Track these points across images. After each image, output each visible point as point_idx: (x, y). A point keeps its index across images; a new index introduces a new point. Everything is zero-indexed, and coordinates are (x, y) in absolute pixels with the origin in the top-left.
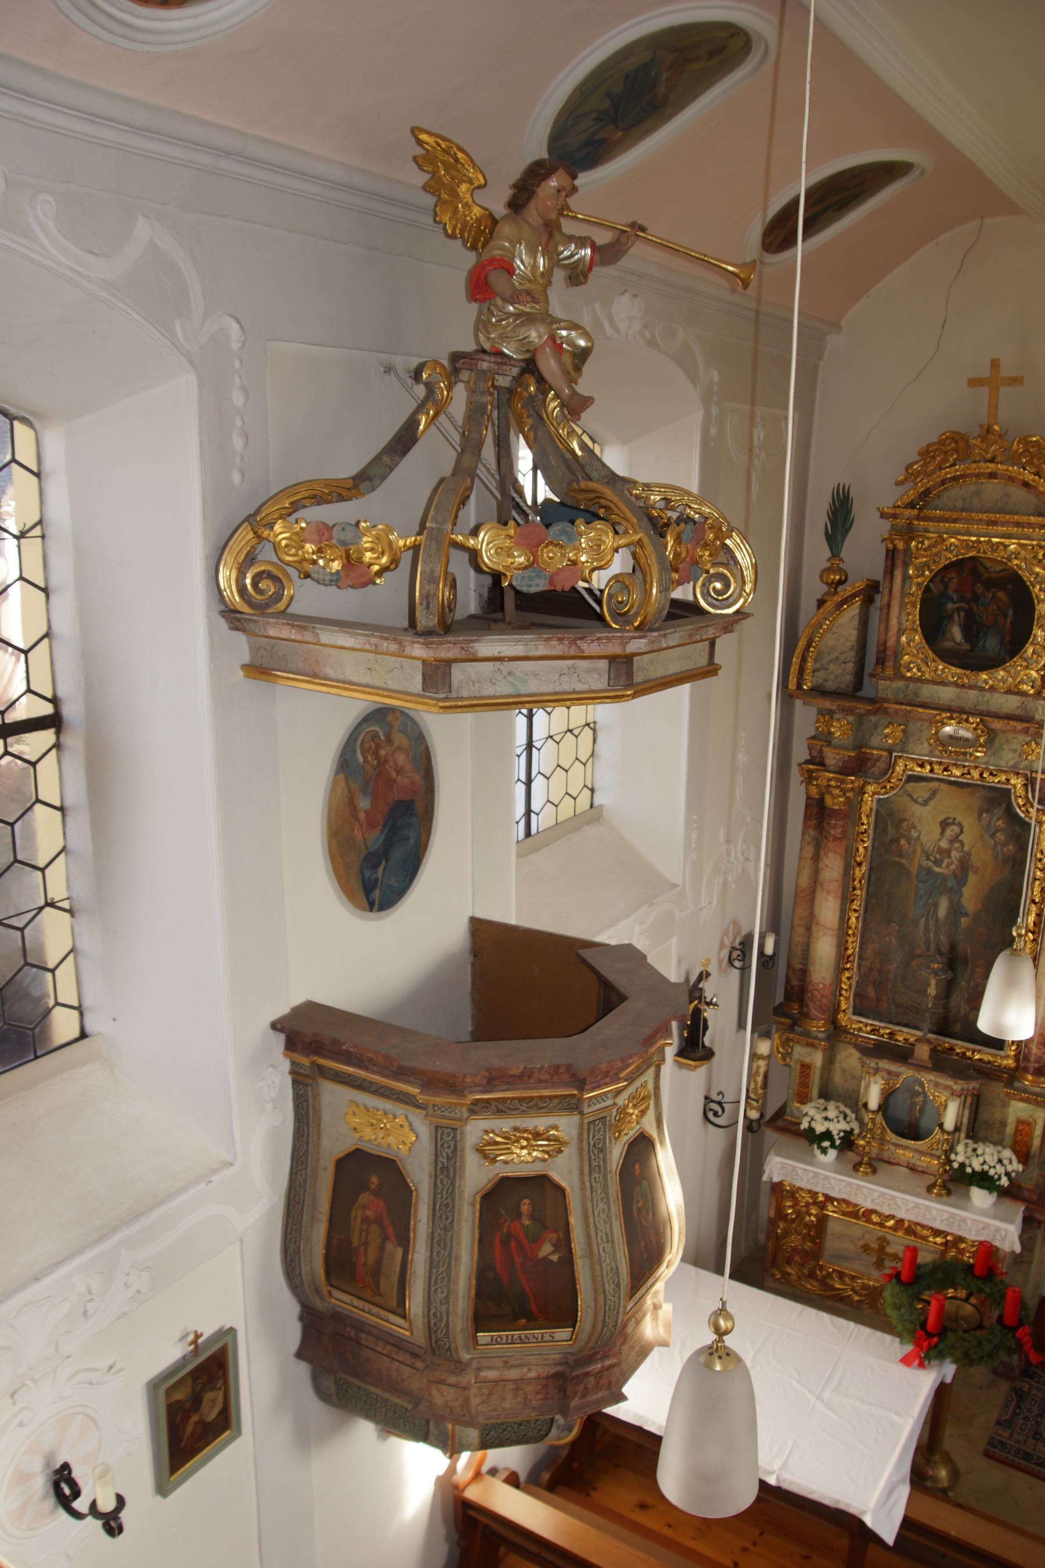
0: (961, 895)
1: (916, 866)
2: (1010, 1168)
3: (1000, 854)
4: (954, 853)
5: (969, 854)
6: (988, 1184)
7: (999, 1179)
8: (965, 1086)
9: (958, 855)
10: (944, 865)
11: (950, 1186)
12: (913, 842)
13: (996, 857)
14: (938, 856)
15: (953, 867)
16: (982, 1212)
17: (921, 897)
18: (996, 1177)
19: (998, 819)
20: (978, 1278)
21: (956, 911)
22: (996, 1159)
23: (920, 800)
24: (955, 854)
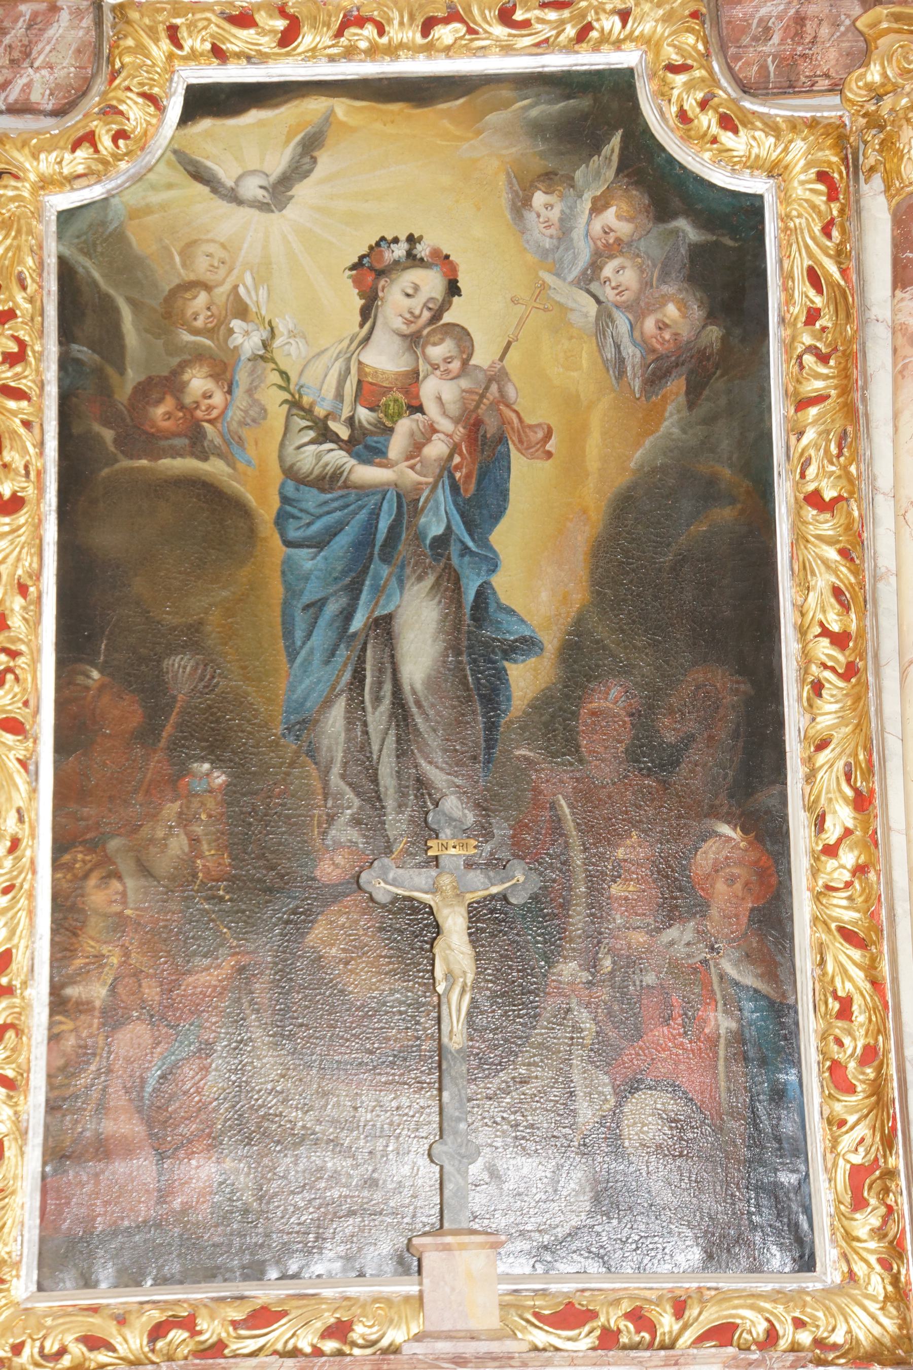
0: (493, 564)
1: (276, 475)
3: (631, 353)
5: (498, 377)
9: (450, 391)
10: (397, 446)
12: (242, 378)
14: (364, 414)
15: (436, 449)
17: (318, 605)
19: (598, 207)
23: (252, 188)
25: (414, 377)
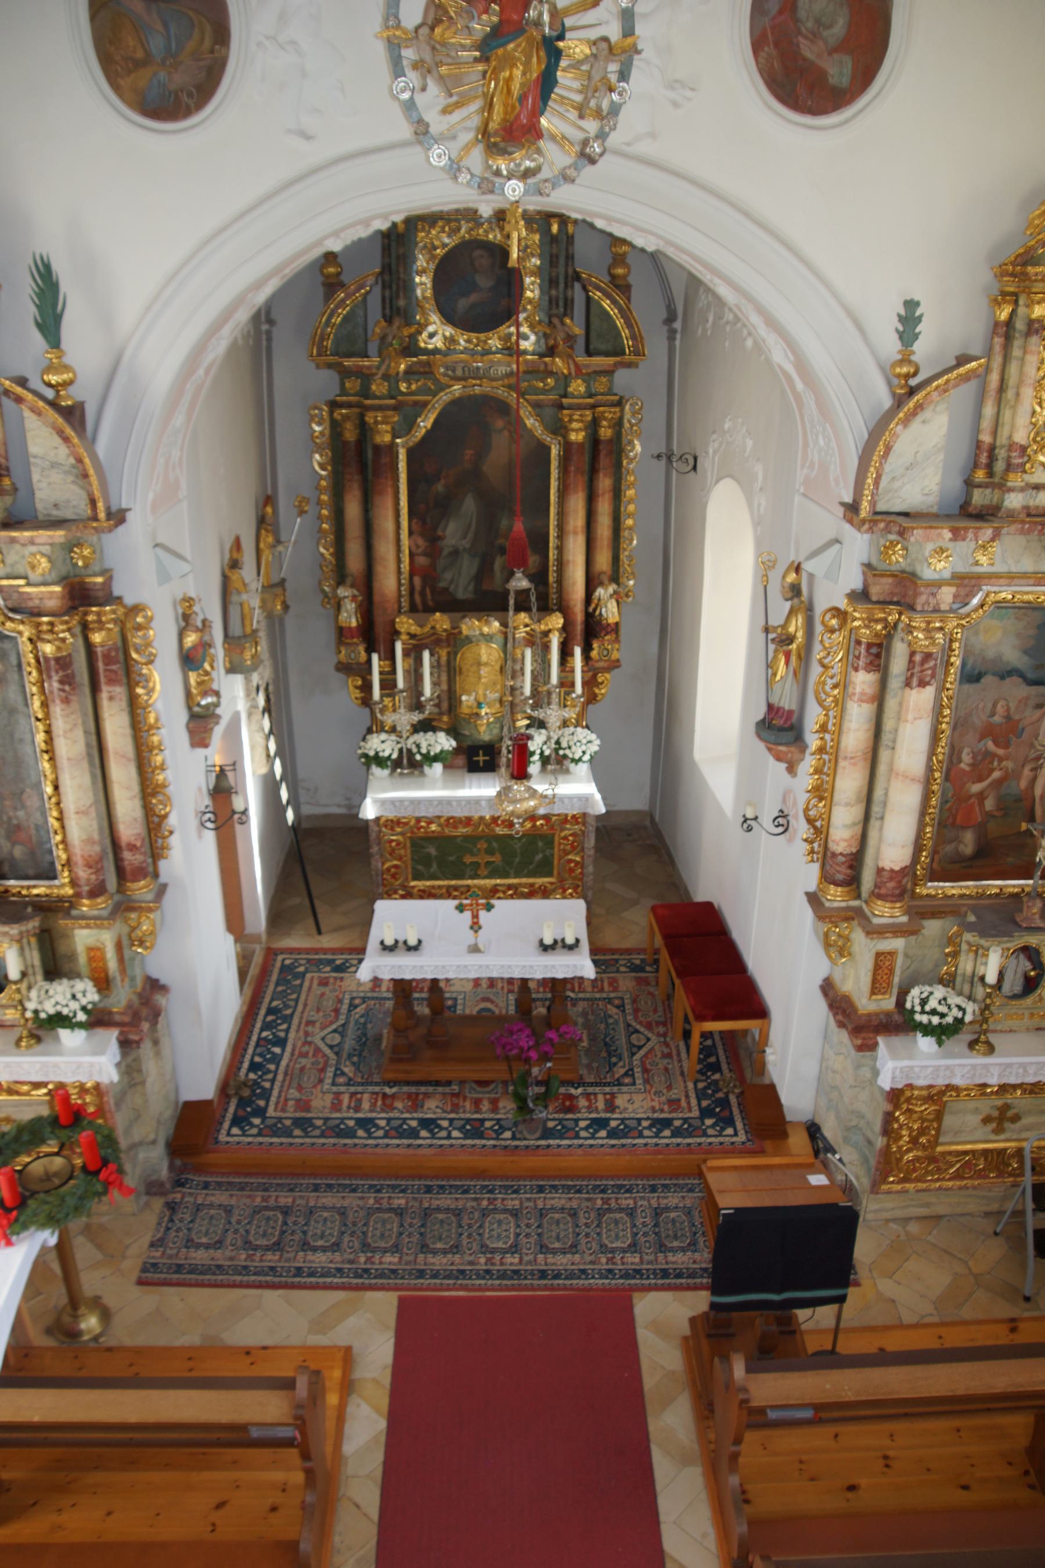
2: (84, 1001)
6: (67, 1023)
7: (75, 1016)
8: (23, 928)
11: (40, 1033)
16: (75, 1052)
18: (71, 1015)
20: (65, 1127)
22: (69, 996)
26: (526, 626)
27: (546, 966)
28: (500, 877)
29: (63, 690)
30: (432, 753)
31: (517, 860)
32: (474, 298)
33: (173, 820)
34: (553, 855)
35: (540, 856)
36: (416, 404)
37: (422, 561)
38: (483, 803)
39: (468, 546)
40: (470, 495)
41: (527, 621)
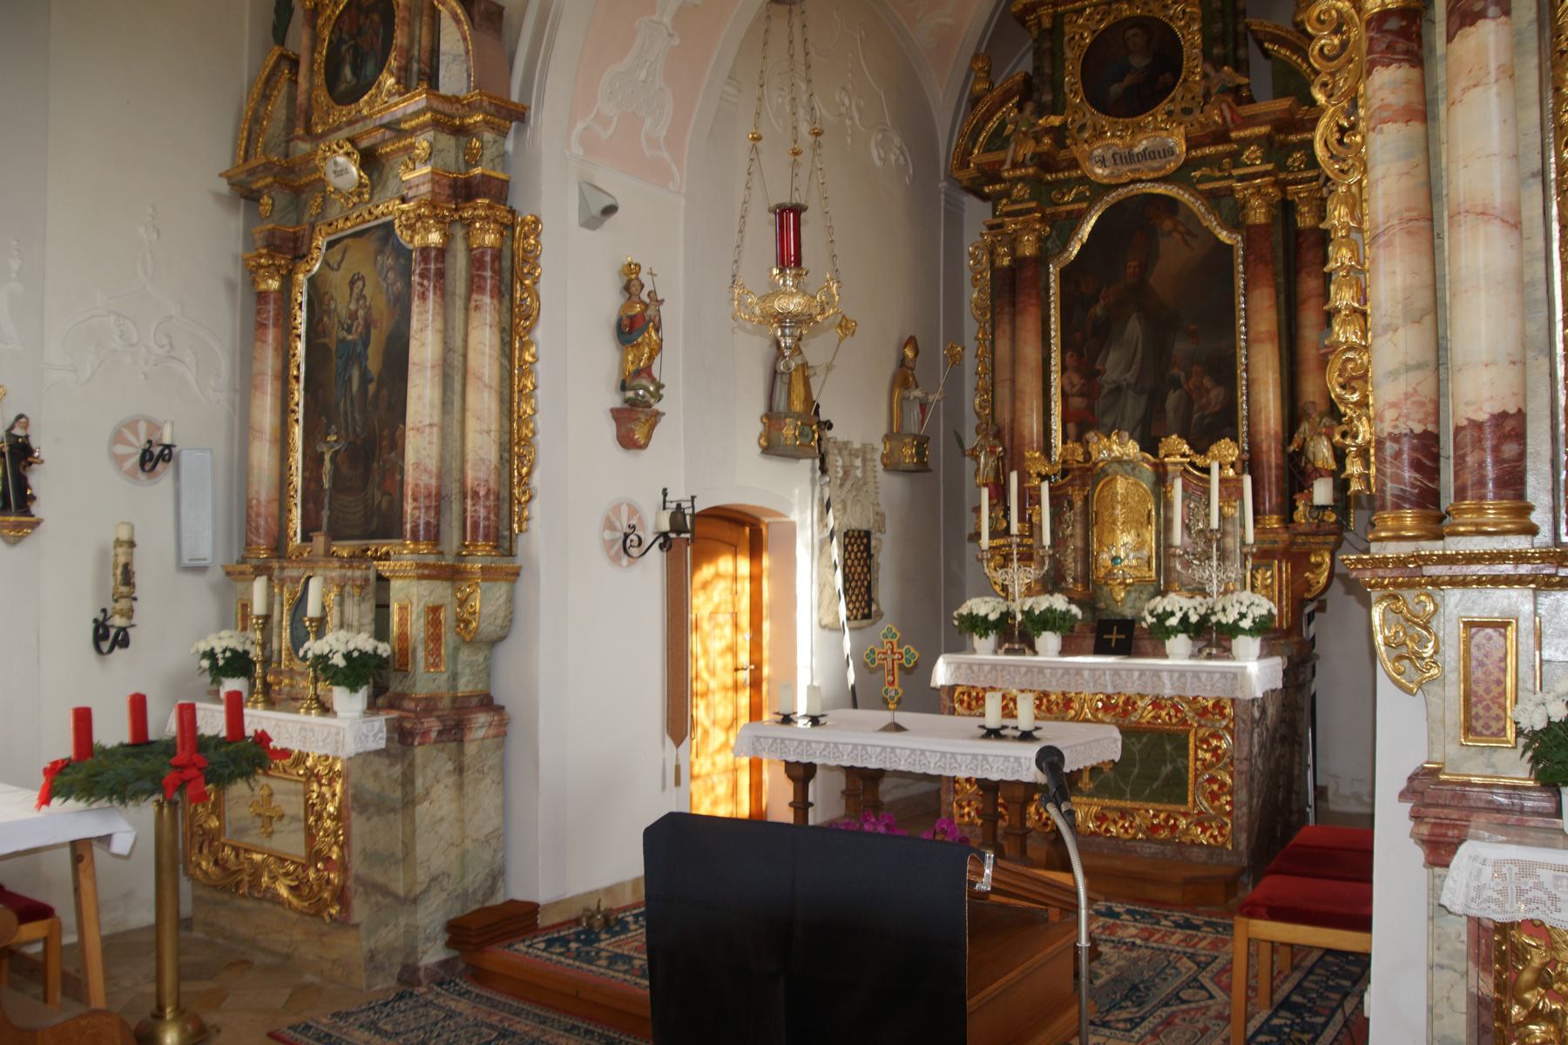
4: (361, 313)
13: (389, 301)
21: (365, 379)
24: (361, 313)
25: (356, 311)
26: (1183, 455)
27: (975, 756)
28: (1111, 797)
29: (421, 285)
30: (1037, 612)
31: (1136, 771)
32: (1128, 80)
33: (536, 480)
34: (1187, 768)
35: (1169, 767)
36: (1069, 213)
37: (1077, 402)
38: (1086, 673)
39: (1133, 380)
40: (1134, 315)
41: (1186, 448)
